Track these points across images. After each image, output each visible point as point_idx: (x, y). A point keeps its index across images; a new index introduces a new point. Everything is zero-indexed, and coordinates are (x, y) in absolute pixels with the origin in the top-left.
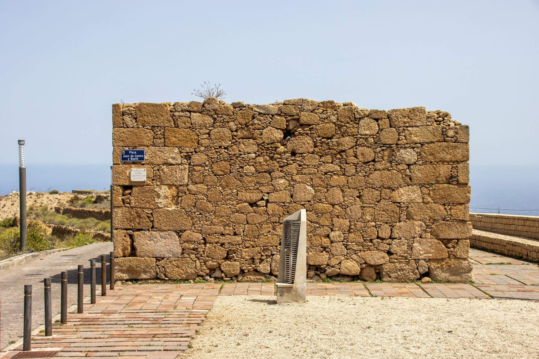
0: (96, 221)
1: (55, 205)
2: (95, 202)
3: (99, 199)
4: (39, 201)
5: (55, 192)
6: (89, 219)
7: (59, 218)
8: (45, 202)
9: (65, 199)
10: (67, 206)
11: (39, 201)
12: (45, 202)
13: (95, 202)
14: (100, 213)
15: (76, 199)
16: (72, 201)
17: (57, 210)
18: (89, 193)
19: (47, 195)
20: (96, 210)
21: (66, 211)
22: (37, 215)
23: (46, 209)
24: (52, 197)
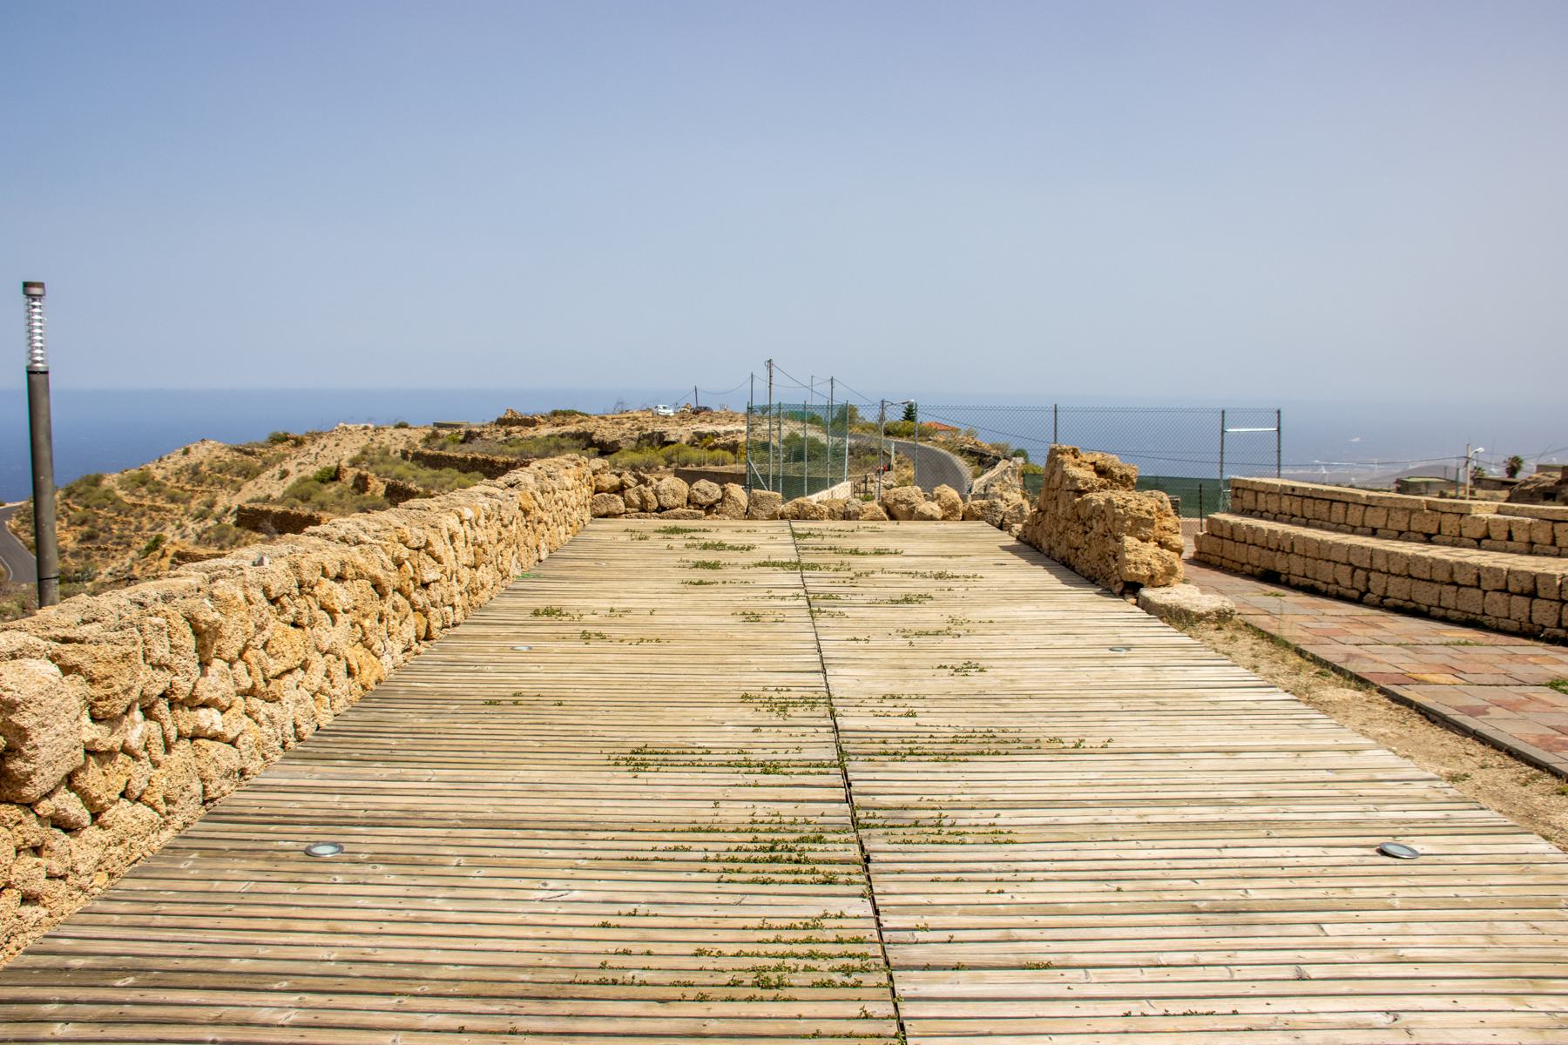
0: (455, 472)
1: (402, 446)
2: (463, 442)
3: (470, 437)
4: (377, 439)
5: (404, 426)
6: (444, 472)
8: (387, 442)
9: (417, 436)
10: (420, 447)
11: (377, 439)
12: (387, 442)
13: (463, 442)
14: (464, 460)
15: (435, 436)
16: (427, 440)
17: (405, 455)
18: (457, 426)
19: (391, 430)
20: (459, 455)
21: (418, 457)
23: (387, 453)
24: (397, 433)
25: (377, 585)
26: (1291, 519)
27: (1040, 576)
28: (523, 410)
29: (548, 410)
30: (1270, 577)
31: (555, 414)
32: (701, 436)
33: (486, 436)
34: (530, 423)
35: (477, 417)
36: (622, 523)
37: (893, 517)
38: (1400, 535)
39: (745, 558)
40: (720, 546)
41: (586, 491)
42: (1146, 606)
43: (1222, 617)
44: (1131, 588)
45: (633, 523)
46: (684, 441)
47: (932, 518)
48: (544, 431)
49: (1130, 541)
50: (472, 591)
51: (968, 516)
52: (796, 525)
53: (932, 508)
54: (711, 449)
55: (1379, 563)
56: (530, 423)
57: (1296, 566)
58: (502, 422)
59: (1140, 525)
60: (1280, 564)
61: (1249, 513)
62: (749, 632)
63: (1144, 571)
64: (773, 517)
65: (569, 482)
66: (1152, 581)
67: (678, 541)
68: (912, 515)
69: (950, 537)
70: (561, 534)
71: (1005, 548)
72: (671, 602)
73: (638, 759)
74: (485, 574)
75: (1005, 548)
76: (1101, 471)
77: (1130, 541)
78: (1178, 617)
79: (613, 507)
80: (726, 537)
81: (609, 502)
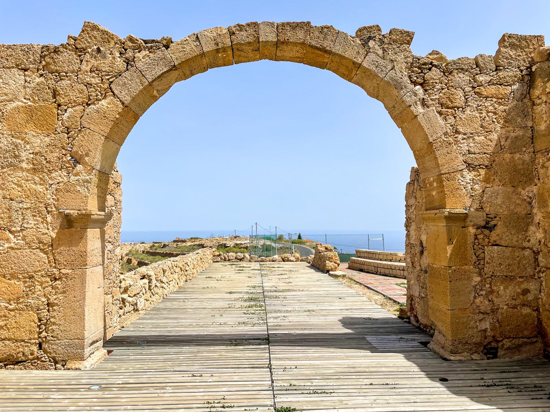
0: (160, 257)
1: (143, 249)
2: (162, 248)
3: (165, 246)
4: (134, 247)
5: (144, 243)
6: (157, 257)
7: (143, 256)
9: (147, 246)
10: (148, 250)
11: (134, 247)
13: (162, 248)
14: (163, 253)
15: (153, 246)
17: (143, 252)
19: (139, 244)
22: (133, 254)
24: (141, 245)
25: (181, 269)
26: (366, 258)
27: (312, 271)
28: (182, 238)
29: (189, 238)
30: (361, 270)
31: (192, 238)
32: (237, 244)
33: (170, 246)
34: (184, 241)
35: (166, 240)
36: (220, 263)
37: (284, 261)
38: (386, 260)
39: (249, 269)
40: (243, 267)
41: (212, 256)
42: (330, 275)
43: (344, 276)
44: (328, 272)
45: (223, 263)
46: (232, 246)
47: (293, 261)
48: (189, 244)
49: (327, 262)
50: (193, 274)
51: (302, 261)
52: (261, 263)
53: (292, 258)
54: (240, 248)
55: (379, 266)
56: (184, 241)
57: (365, 267)
58: (175, 241)
59: (330, 259)
60: (363, 267)
61: (359, 257)
62: (249, 279)
63: (330, 268)
64: (256, 261)
65: (209, 253)
66: (332, 270)
67: (234, 266)
68: (289, 260)
69: (296, 265)
70: (207, 265)
71: (308, 267)
72: (234, 276)
73: (230, 293)
74: (195, 271)
75: (308, 267)
76: (326, 248)
77: (327, 262)
78: (336, 276)
79: (218, 260)
80: (245, 265)
81: (217, 259)
